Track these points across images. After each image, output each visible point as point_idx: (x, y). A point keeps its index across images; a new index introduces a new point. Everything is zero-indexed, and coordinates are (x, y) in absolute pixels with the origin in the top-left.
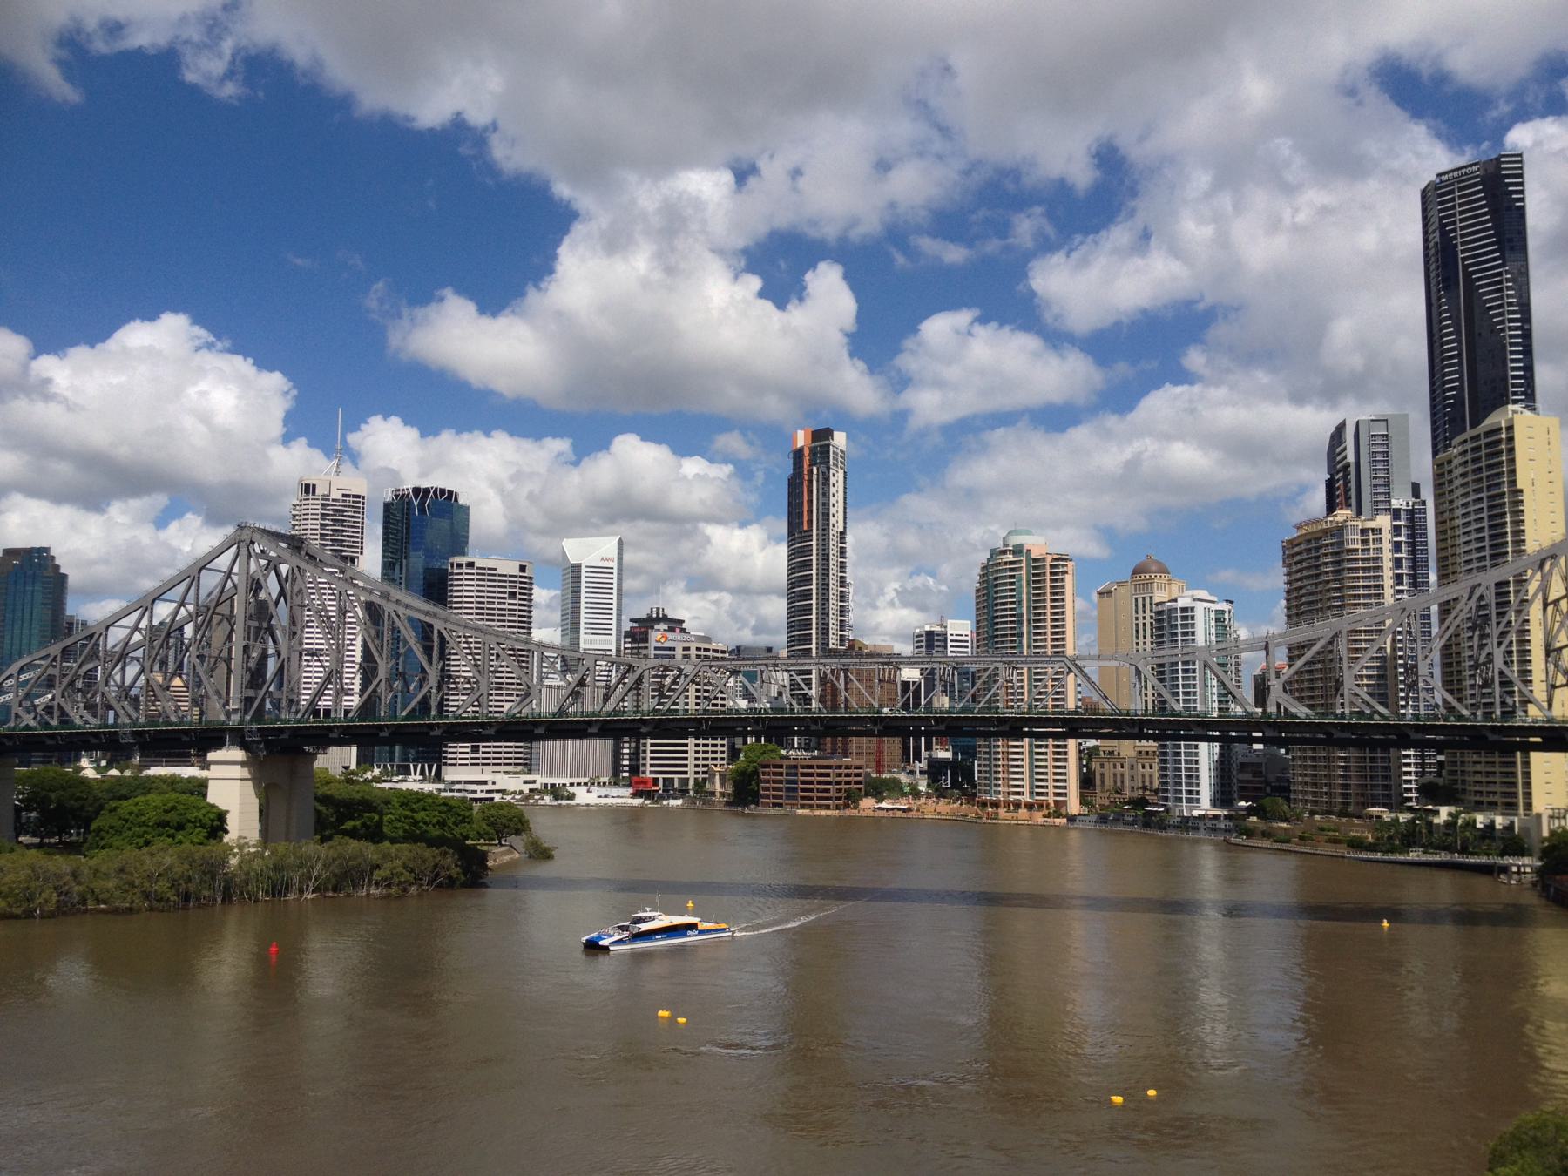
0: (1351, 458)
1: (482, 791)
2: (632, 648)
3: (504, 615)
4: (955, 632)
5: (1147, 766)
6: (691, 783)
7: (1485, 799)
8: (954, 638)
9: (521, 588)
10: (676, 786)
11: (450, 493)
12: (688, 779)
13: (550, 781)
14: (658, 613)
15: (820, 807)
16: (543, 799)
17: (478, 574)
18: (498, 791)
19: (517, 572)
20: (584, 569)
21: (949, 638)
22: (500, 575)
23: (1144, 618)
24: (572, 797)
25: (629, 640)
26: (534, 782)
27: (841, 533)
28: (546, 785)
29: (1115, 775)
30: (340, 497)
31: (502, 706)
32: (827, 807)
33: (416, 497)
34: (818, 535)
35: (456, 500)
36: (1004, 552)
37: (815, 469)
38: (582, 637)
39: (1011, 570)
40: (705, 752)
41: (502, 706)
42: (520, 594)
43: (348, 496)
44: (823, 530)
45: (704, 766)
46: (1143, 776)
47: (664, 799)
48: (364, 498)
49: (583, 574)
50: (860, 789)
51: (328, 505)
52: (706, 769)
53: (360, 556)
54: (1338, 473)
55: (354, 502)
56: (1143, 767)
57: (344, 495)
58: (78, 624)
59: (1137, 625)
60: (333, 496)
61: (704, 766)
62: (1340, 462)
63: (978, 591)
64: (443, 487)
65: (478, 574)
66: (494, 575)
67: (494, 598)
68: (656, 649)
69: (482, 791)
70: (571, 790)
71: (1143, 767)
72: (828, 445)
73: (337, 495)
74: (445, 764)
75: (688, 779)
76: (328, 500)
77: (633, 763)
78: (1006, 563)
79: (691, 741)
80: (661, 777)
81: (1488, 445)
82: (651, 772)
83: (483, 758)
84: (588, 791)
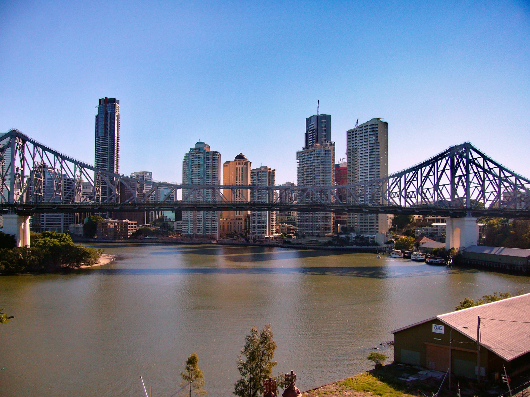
0: (315, 127)
4: (146, 176)
5: (240, 223)
7: (363, 230)
8: (145, 178)
21: (145, 178)
23: (240, 174)
29: (228, 226)
36: (196, 149)
39: (199, 155)
40: (70, 219)
46: (238, 226)
54: (309, 131)
56: (238, 223)
59: (237, 176)
62: (311, 128)
63: (183, 162)
71: (238, 223)
78: (197, 153)
79: (63, 214)
81: (369, 129)
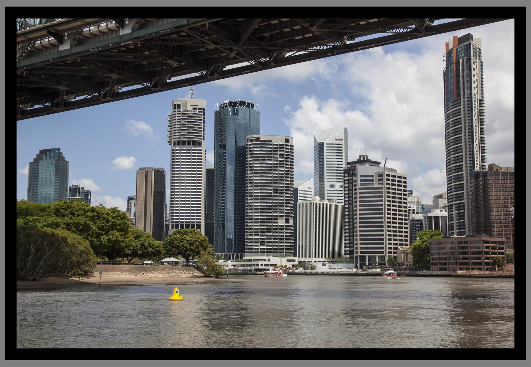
1: (262, 265)
2: (348, 180)
3: (277, 167)
6: (387, 259)
9: (286, 152)
10: (377, 260)
11: (249, 104)
12: (384, 257)
13: (303, 260)
14: (364, 158)
15: (473, 269)
16: (297, 269)
17: (262, 144)
18: (272, 265)
19: (283, 143)
20: (325, 145)
22: (274, 145)
24: (313, 268)
25: (346, 175)
26: (294, 261)
27: (480, 100)
28: (300, 262)
30: (192, 110)
31: (277, 219)
32: (480, 269)
33: (230, 106)
34: (464, 101)
35: (252, 107)
37: (461, 60)
38: (326, 183)
41: (277, 219)
42: (286, 155)
43: (196, 109)
44: (468, 98)
45: (394, 248)
47: (369, 268)
48: (204, 110)
49: (325, 148)
50: (503, 258)
51: (186, 114)
52: (395, 251)
53: (203, 141)
55: (199, 112)
57: (194, 109)
58: (79, 189)
60: (187, 110)
61: (394, 248)
64: (244, 101)
65: (262, 144)
66: (271, 145)
67: (271, 157)
68: (361, 176)
69: (262, 265)
70: (313, 264)
72: (470, 44)
73: (190, 108)
74: (247, 252)
75: (384, 257)
76: (186, 111)
77: (351, 249)
80: (367, 255)
82: (361, 252)
83: (267, 249)
84: (323, 265)
